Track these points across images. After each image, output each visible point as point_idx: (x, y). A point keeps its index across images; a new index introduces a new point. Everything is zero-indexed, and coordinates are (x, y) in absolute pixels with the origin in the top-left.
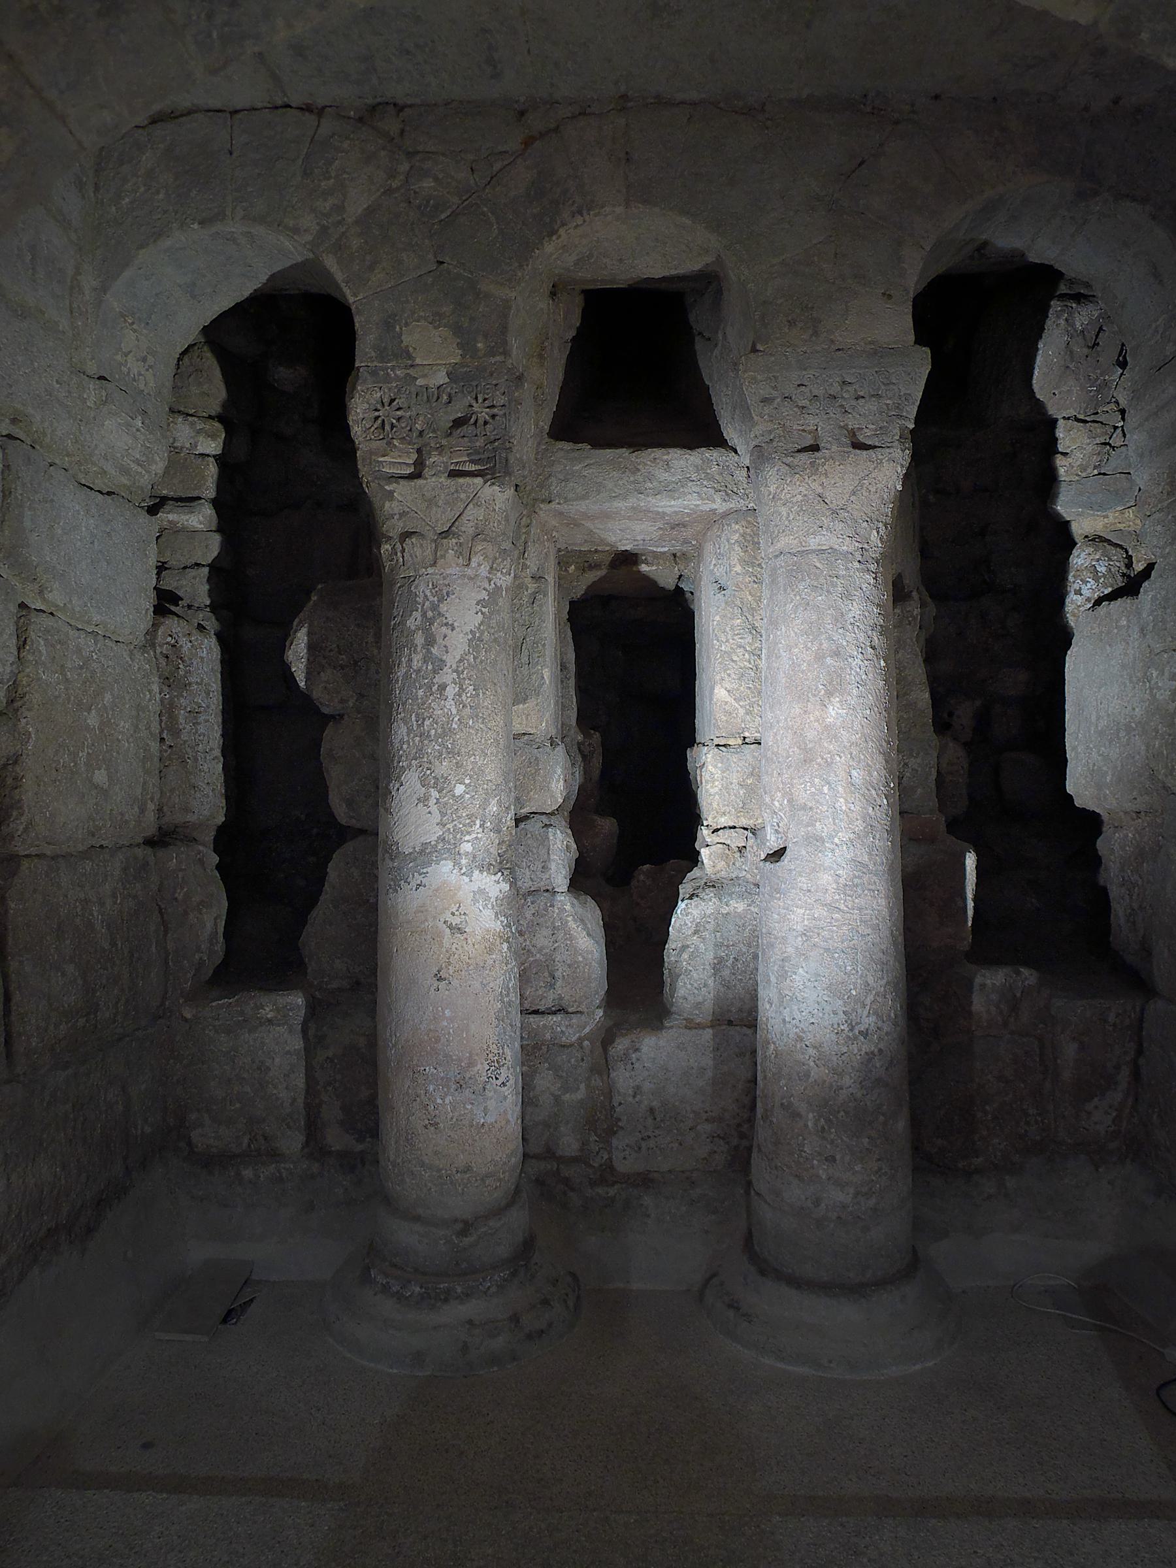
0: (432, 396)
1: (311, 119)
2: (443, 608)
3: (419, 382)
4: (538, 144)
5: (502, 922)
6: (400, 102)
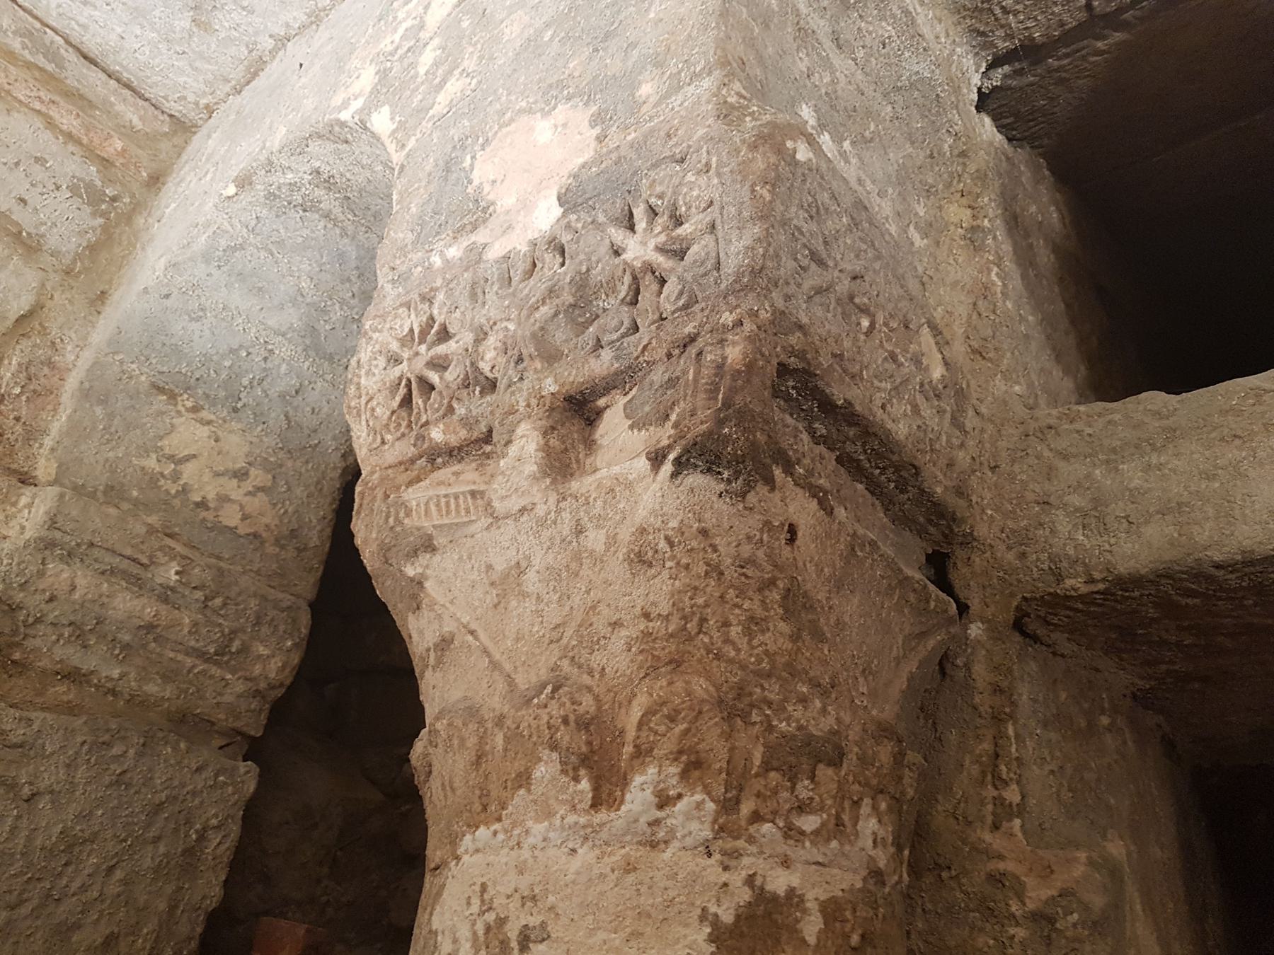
3: (495, 252)
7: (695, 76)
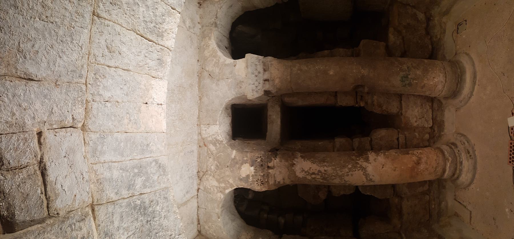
1: (200, 190)
2: (306, 170)
3: (253, 173)
4: (206, 143)
5: (381, 154)
6: (197, 171)
7: (247, 155)
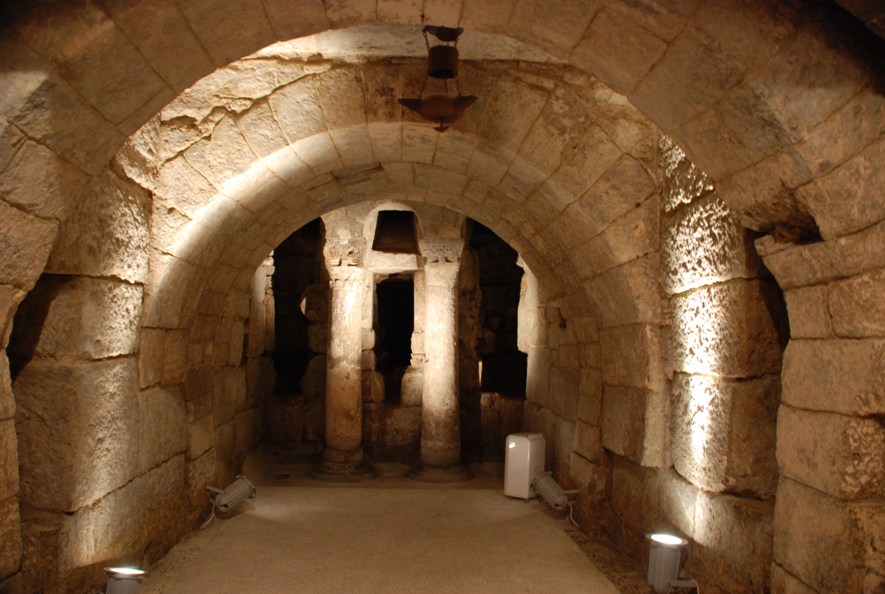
0: (344, 247)
